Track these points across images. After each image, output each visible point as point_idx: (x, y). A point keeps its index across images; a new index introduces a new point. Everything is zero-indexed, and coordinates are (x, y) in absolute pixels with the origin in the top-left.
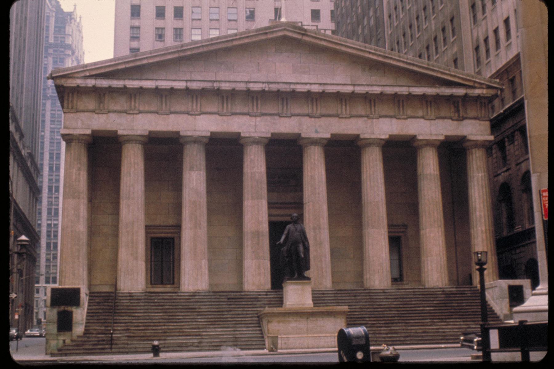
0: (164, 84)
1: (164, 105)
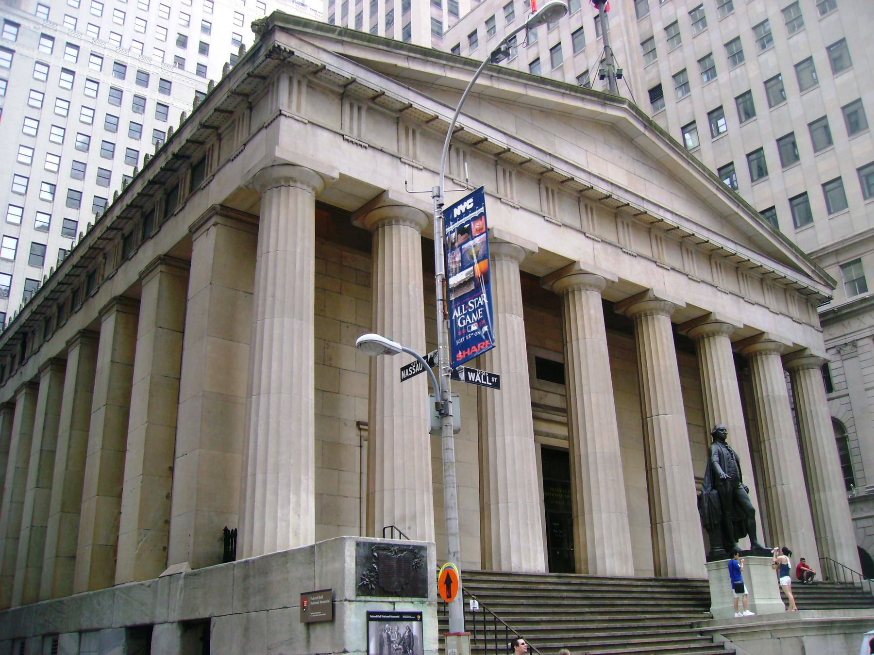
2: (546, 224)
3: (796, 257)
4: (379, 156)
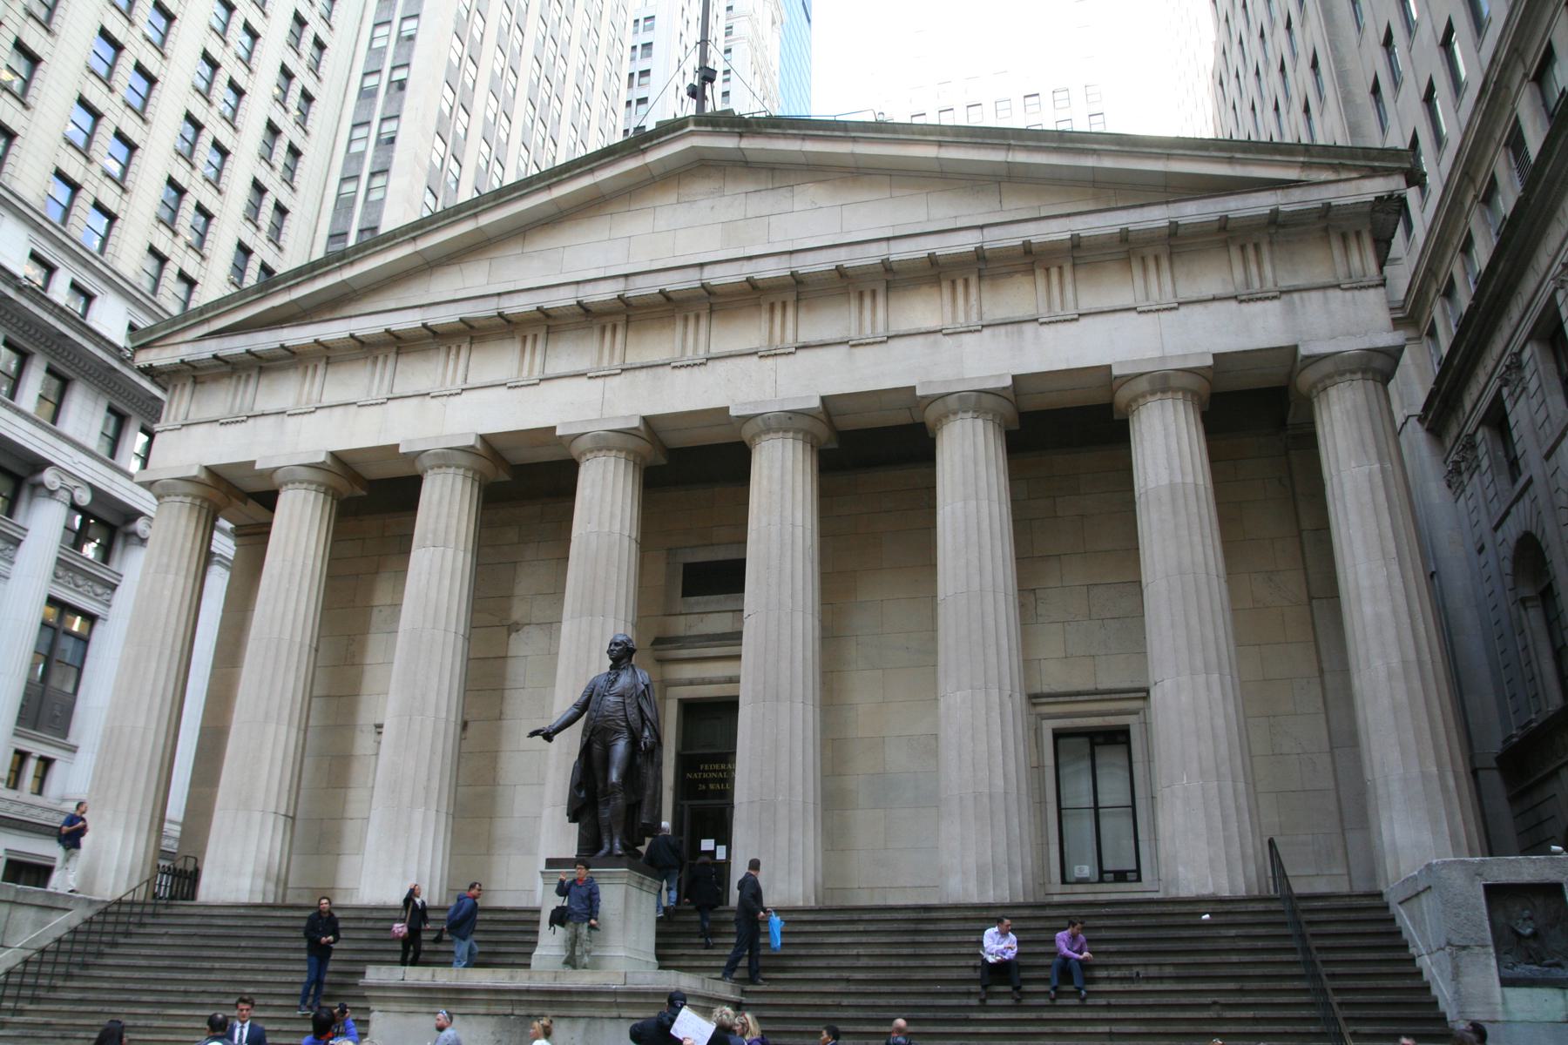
0: (367, 326)
3: (1231, 161)
4: (260, 420)
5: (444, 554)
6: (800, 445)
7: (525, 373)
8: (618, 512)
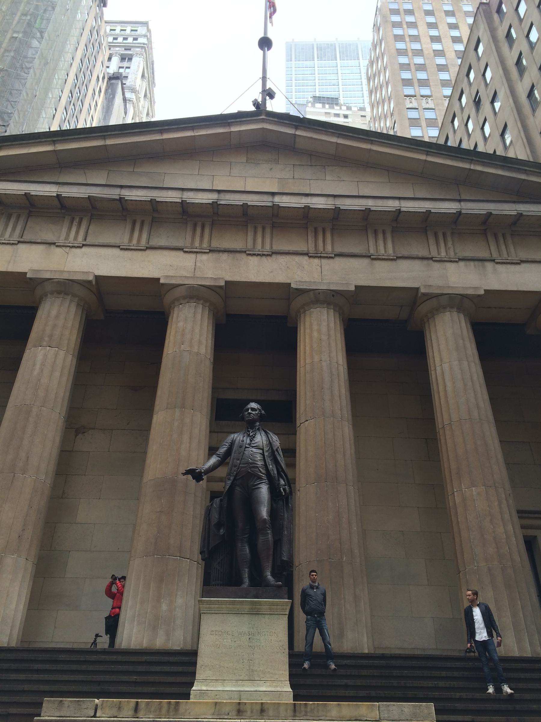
1: (9, 229)
2: (122, 252)
5: (56, 355)
6: (337, 316)
7: (135, 241)
8: (204, 342)
